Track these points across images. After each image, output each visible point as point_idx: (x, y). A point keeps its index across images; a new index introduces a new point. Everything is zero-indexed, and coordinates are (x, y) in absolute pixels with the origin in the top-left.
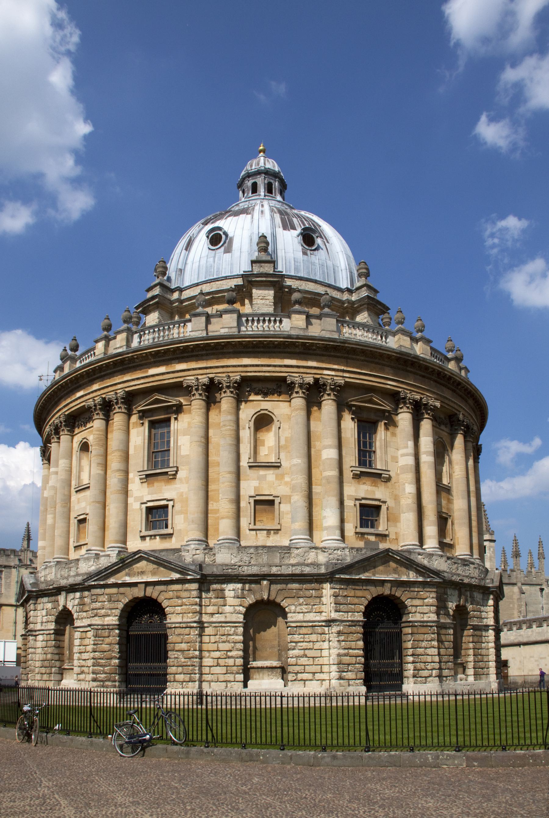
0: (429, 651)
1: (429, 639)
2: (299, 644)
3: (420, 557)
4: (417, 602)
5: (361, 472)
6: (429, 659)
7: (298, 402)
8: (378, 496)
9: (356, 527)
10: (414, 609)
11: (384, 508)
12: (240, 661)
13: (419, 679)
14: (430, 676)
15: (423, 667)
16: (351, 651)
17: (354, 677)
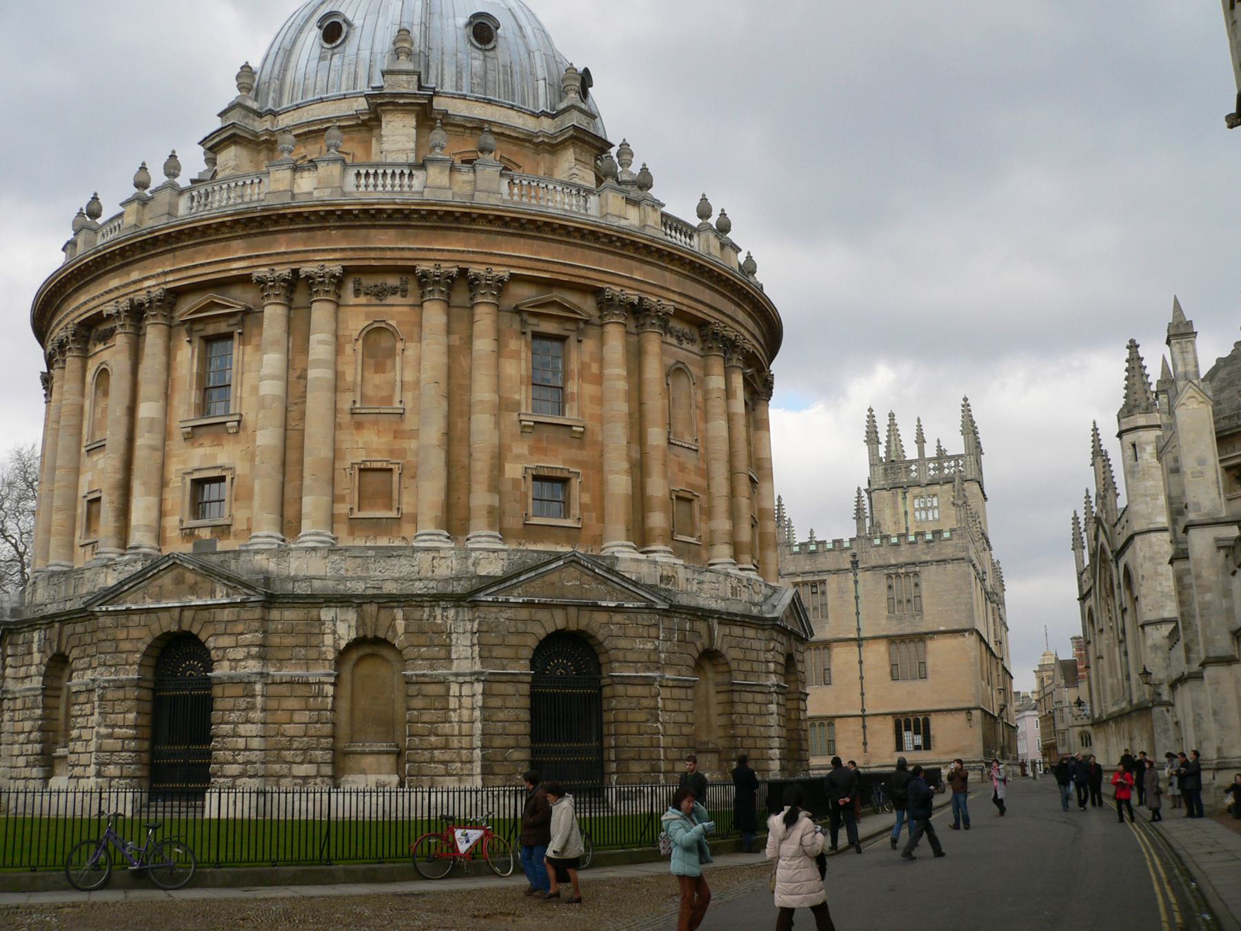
0: (242, 729)
1: (243, 706)
2: (79, 720)
3: (258, 557)
4: (225, 641)
5: (194, 427)
6: (241, 743)
7: (120, 340)
8: (219, 463)
9: (181, 521)
10: (220, 653)
11: (228, 479)
12: (38, 747)
13: (222, 780)
14: (241, 775)
15: (230, 758)
16: (117, 730)
17: (118, 773)
